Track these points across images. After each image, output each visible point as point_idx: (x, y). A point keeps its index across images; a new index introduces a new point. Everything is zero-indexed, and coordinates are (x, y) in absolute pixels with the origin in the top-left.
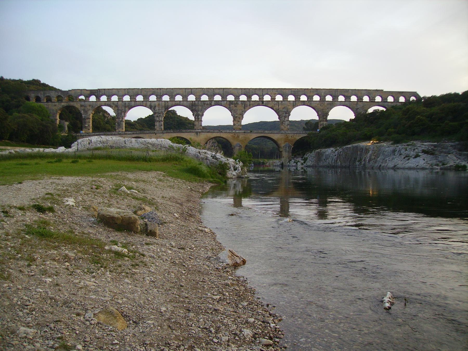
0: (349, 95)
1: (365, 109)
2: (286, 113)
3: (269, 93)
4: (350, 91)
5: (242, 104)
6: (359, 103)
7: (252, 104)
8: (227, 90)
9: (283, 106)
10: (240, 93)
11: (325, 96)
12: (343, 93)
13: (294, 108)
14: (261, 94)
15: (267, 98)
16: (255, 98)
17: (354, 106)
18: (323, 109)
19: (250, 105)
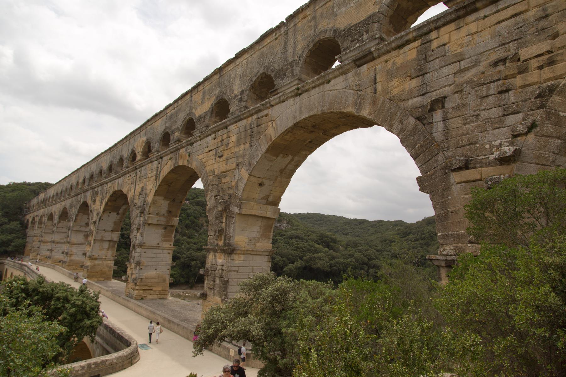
9: (141, 186)
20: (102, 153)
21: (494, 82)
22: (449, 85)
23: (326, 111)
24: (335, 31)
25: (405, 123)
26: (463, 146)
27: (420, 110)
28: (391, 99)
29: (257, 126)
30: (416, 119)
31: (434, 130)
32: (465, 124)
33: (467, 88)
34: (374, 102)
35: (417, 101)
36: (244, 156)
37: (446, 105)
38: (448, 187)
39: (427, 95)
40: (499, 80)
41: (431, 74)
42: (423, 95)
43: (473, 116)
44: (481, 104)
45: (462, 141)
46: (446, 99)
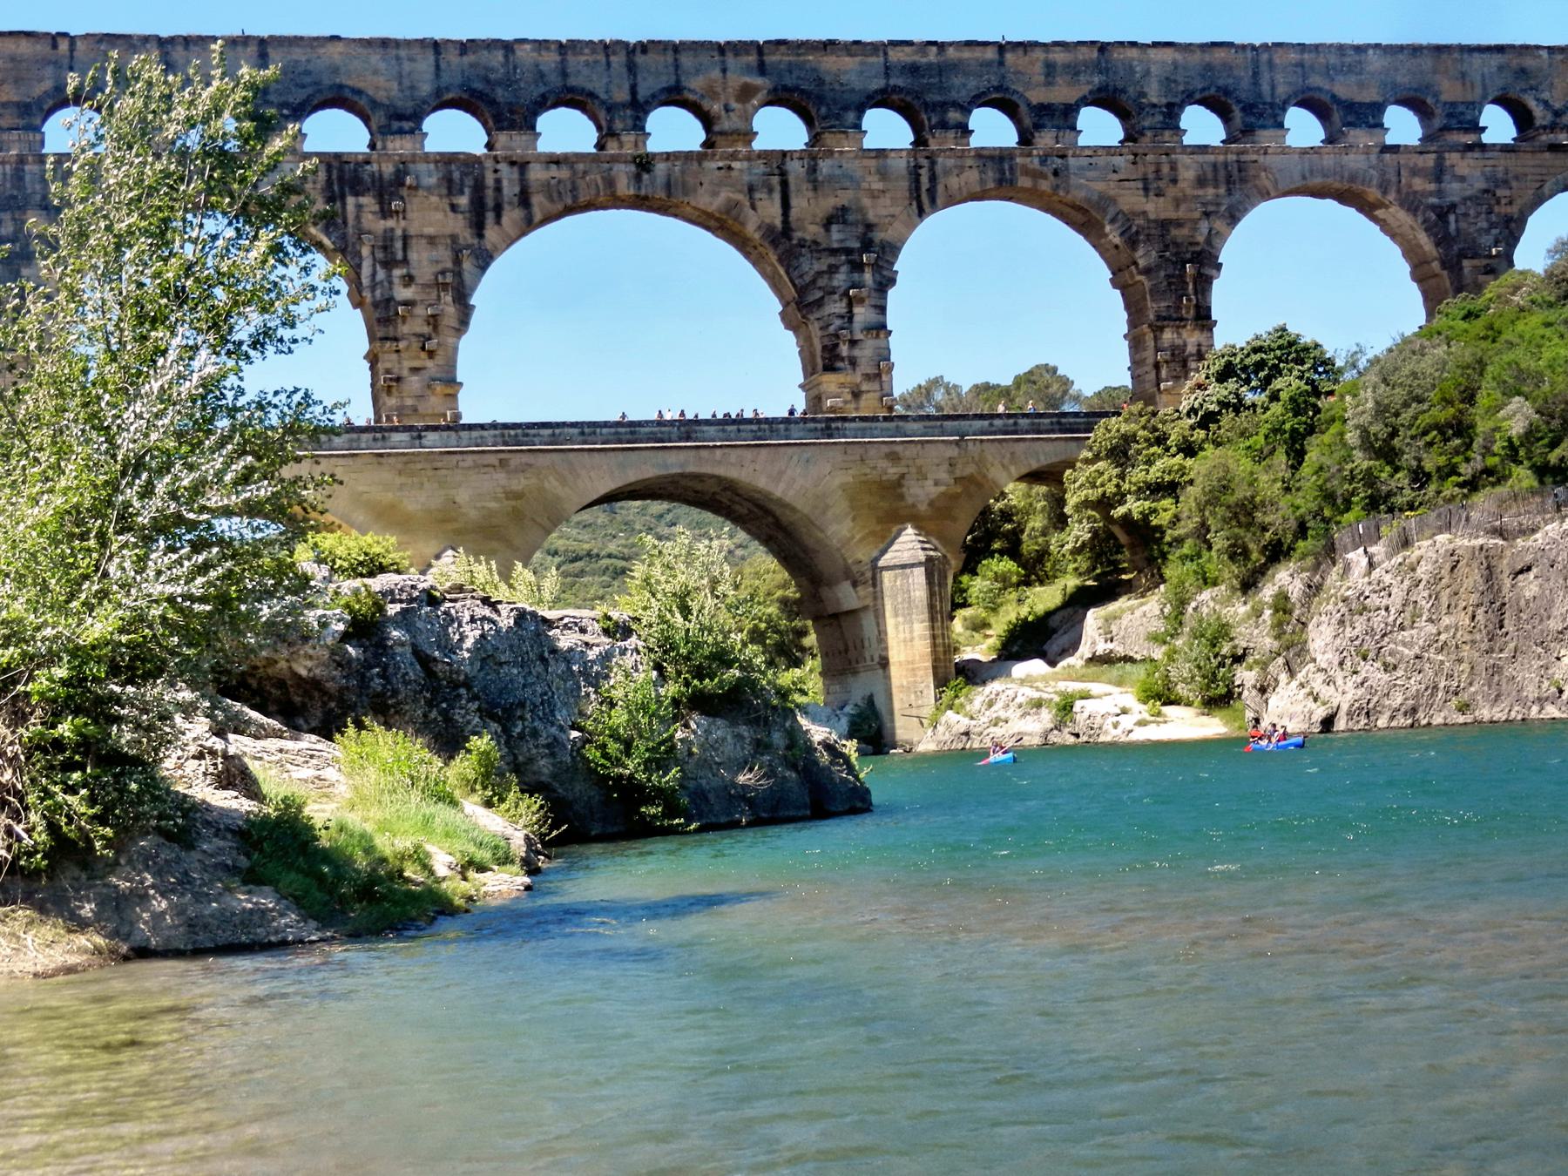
0: (1370, 95)
1: (1503, 209)
2: (858, 267)
3: (695, 85)
4: (1375, 62)
5: (450, 187)
6: (1453, 158)
7: (549, 189)
8: (298, 54)
9: (829, 203)
10: (426, 89)
11: (1171, 114)
12: (1316, 80)
13: (922, 213)
14: (622, 95)
15: (672, 131)
16: (565, 132)
17: (1419, 184)
18: (1165, 225)
19: (524, 200)
20: (335, 38)
24: (1334, 96)
29: (1240, 171)
34: (1399, 191)
35: (1433, 200)
36: (1218, 204)
38: (1461, 269)
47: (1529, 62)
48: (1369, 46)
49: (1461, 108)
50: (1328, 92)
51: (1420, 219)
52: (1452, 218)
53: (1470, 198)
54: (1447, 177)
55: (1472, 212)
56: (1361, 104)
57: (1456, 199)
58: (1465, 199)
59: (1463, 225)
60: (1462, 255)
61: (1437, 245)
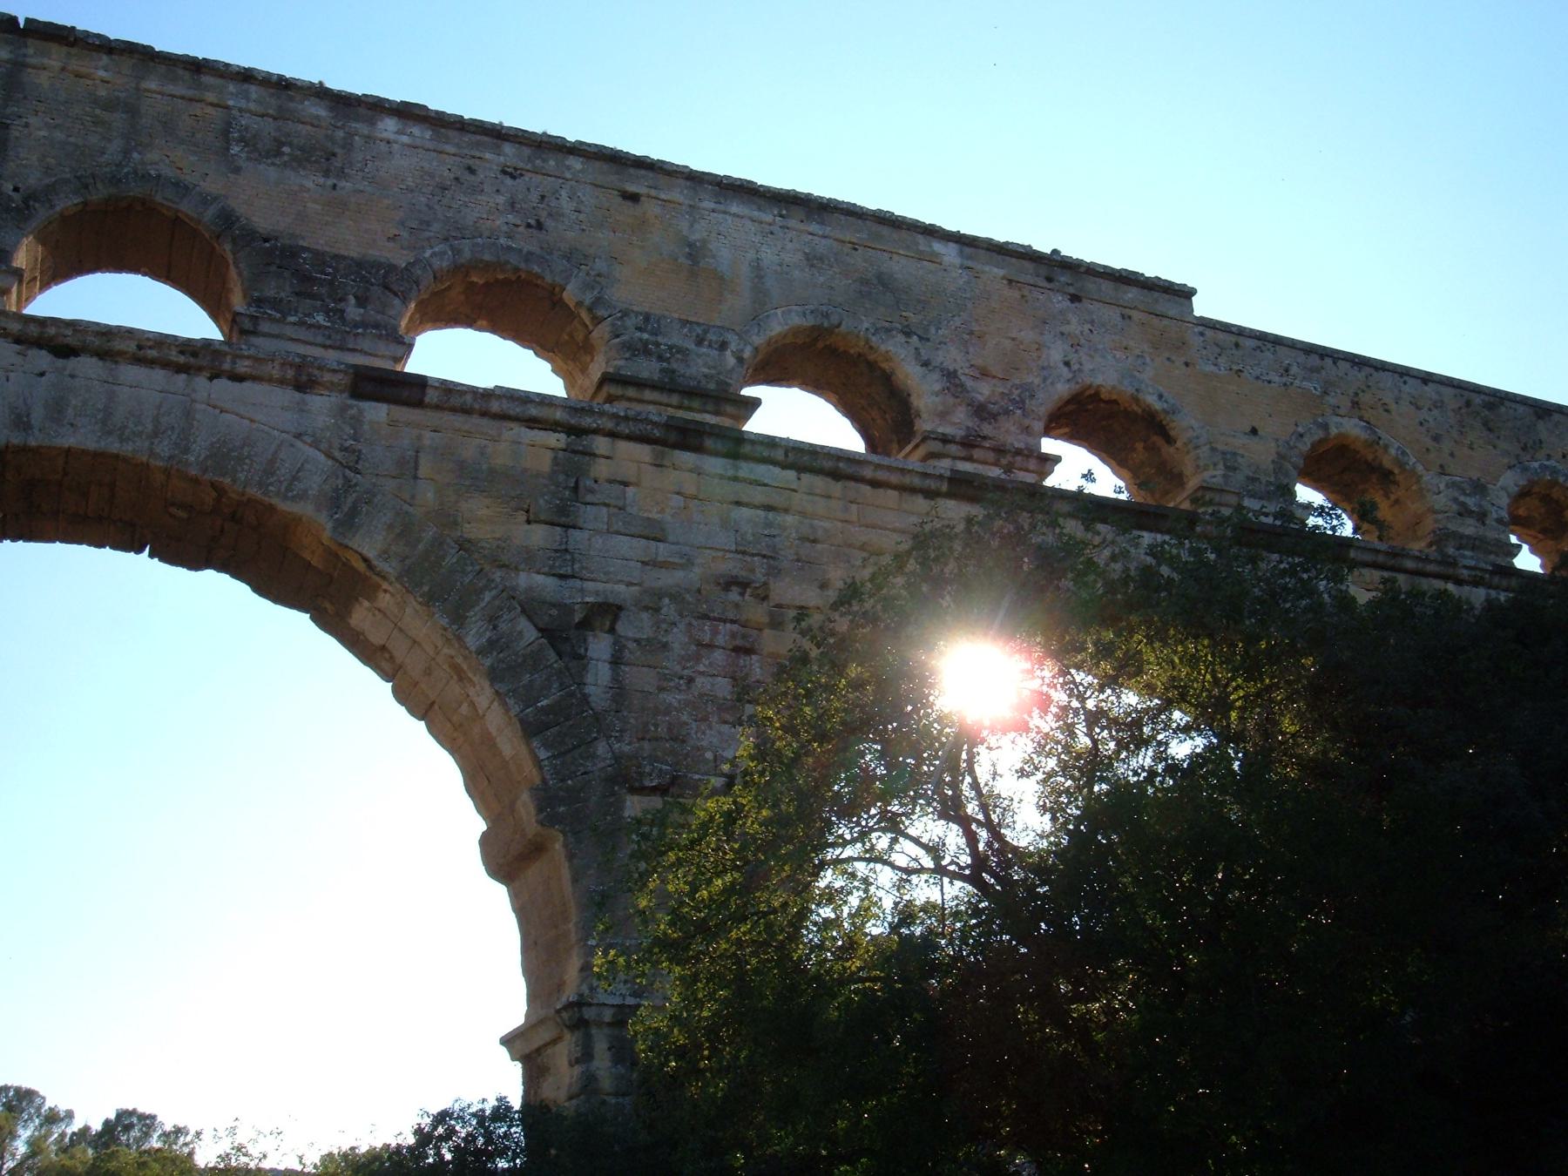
21: (725, 621)
22: (629, 584)
23: (193, 472)
24: (228, 219)
25: (503, 627)
26: (656, 739)
27: (554, 612)
28: (467, 545)
30: (540, 630)
31: (589, 678)
32: (661, 689)
33: (668, 609)
37: (620, 627)
39: (571, 582)
40: (733, 622)
41: (586, 534)
42: (562, 577)
43: (681, 678)
44: (697, 658)
45: (656, 726)
46: (622, 614)
47: (901, 267)
48: (376, 107)
49: (676, 338)
50: (206, 200)
51: (475, 635)
52: (599, 647)
53: (676, 597)
54: (593, 516)
55: (678, 639)
56: (320, 258)
57: (621, 592)
58: (652, 602)
59: (640, 678)
60: (624, 778)
61: (531, 729)
